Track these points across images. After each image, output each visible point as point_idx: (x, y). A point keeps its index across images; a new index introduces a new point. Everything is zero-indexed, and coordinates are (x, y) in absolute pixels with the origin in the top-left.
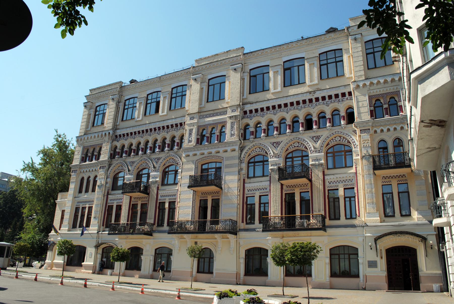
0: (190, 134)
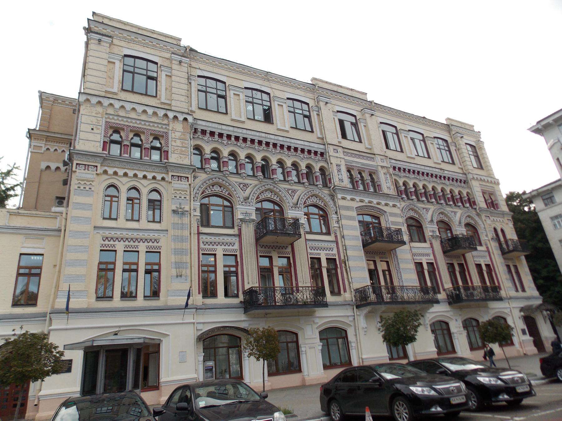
0: (339, 171)
